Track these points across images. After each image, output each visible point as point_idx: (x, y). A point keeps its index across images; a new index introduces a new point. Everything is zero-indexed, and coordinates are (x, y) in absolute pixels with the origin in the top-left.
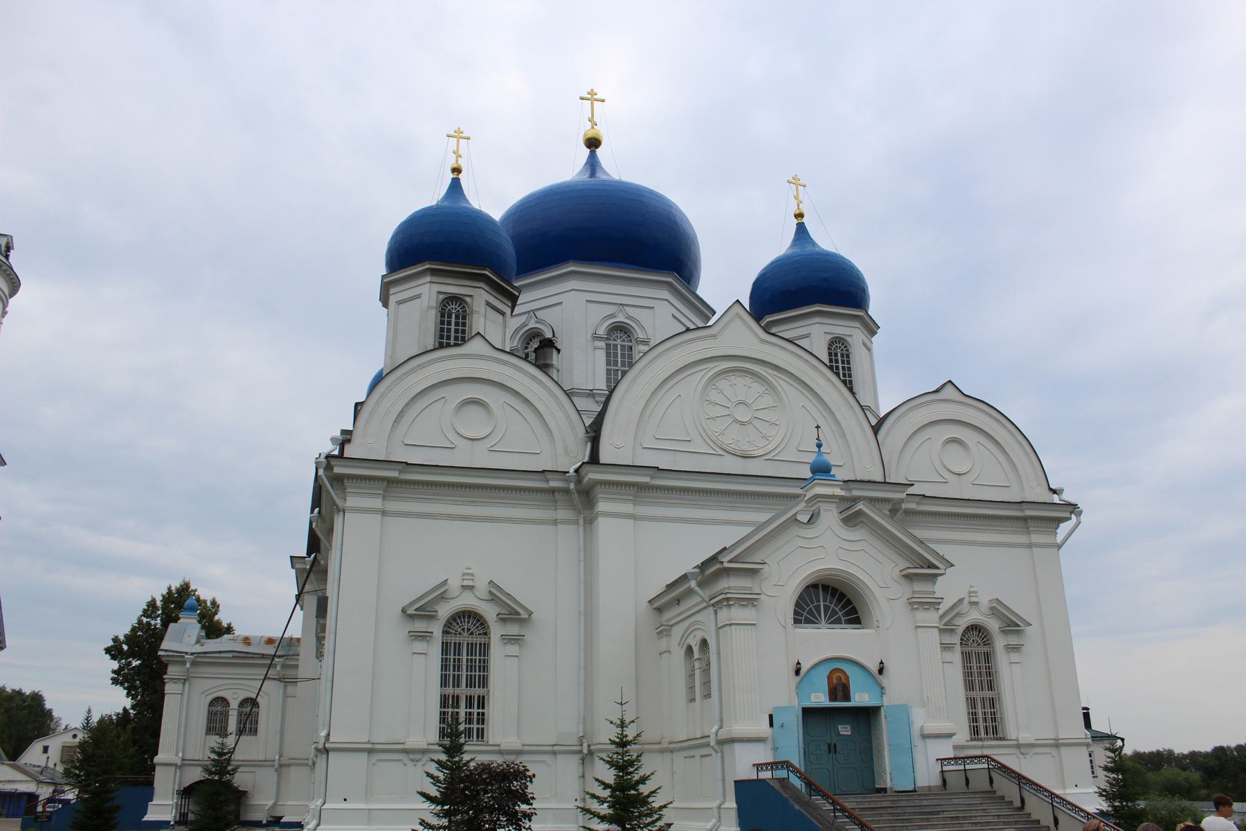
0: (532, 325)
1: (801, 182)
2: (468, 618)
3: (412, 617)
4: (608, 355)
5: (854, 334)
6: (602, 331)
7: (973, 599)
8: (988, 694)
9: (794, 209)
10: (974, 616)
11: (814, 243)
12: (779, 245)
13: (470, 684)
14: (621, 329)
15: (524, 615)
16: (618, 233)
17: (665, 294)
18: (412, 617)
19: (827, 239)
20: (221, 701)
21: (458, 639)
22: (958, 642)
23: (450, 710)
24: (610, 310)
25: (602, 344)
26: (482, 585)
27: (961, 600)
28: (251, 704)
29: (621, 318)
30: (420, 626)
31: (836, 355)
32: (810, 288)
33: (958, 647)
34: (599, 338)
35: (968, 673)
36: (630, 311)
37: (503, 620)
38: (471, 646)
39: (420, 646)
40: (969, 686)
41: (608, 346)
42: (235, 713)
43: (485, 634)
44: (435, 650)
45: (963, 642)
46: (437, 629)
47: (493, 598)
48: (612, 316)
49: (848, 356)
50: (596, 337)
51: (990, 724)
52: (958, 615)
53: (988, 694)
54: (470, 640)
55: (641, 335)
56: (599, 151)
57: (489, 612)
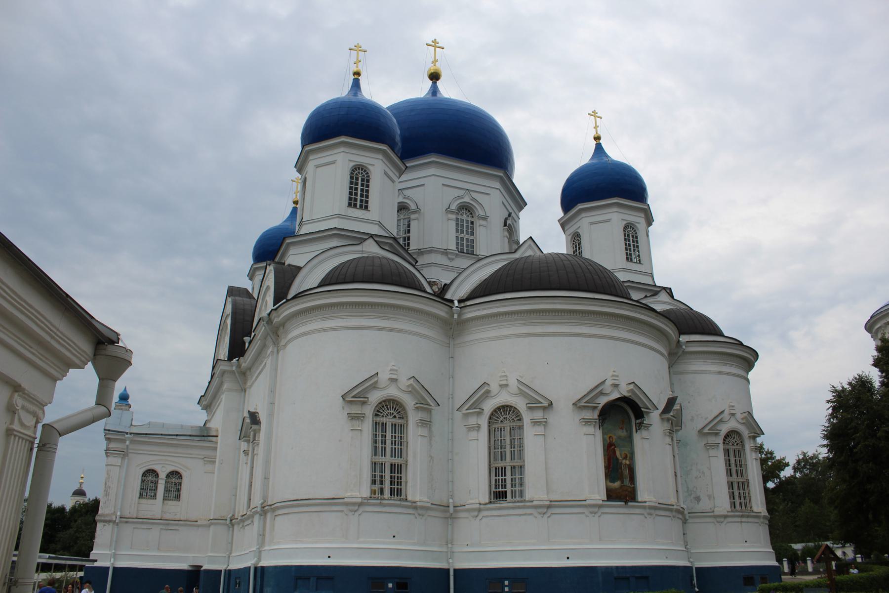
2: (391, 406)
3: (351, 402)
4: (457, 225)
6: (454, 207)
7: (732, 412)
9: (593, 133)
10: (732, 425)
11: (607, 156)
12: (582, 157)
13: (393, 454)
14: (466, 208)
16: (462, 139)
18: (351, 402)
19: (616, 153)
20: (151, 473)
21: (384, 420)
22: (721, 441)
25: (454, 217)
26: (404, 382)
27: (722, 412)
28: (175, 475)
29: (467, 199)
30: (356, 410)
32: (605, 185)
33: (721, 445)
34: (452, 212)
35: (728, 463)
36: (474, 195)
38: (394, 426)
39: (356, 424)
40: (729, 473)
41: (457, 219)
42: (164, 482)
44: (367, 427)
46: (369, 411)
47: (412, 391)
48: (461, 197)
50: (448, 210)
52: (721, 421)
53: (740, 479)
54: (395, 421)
55: (481, 213)
56: (439, 83)
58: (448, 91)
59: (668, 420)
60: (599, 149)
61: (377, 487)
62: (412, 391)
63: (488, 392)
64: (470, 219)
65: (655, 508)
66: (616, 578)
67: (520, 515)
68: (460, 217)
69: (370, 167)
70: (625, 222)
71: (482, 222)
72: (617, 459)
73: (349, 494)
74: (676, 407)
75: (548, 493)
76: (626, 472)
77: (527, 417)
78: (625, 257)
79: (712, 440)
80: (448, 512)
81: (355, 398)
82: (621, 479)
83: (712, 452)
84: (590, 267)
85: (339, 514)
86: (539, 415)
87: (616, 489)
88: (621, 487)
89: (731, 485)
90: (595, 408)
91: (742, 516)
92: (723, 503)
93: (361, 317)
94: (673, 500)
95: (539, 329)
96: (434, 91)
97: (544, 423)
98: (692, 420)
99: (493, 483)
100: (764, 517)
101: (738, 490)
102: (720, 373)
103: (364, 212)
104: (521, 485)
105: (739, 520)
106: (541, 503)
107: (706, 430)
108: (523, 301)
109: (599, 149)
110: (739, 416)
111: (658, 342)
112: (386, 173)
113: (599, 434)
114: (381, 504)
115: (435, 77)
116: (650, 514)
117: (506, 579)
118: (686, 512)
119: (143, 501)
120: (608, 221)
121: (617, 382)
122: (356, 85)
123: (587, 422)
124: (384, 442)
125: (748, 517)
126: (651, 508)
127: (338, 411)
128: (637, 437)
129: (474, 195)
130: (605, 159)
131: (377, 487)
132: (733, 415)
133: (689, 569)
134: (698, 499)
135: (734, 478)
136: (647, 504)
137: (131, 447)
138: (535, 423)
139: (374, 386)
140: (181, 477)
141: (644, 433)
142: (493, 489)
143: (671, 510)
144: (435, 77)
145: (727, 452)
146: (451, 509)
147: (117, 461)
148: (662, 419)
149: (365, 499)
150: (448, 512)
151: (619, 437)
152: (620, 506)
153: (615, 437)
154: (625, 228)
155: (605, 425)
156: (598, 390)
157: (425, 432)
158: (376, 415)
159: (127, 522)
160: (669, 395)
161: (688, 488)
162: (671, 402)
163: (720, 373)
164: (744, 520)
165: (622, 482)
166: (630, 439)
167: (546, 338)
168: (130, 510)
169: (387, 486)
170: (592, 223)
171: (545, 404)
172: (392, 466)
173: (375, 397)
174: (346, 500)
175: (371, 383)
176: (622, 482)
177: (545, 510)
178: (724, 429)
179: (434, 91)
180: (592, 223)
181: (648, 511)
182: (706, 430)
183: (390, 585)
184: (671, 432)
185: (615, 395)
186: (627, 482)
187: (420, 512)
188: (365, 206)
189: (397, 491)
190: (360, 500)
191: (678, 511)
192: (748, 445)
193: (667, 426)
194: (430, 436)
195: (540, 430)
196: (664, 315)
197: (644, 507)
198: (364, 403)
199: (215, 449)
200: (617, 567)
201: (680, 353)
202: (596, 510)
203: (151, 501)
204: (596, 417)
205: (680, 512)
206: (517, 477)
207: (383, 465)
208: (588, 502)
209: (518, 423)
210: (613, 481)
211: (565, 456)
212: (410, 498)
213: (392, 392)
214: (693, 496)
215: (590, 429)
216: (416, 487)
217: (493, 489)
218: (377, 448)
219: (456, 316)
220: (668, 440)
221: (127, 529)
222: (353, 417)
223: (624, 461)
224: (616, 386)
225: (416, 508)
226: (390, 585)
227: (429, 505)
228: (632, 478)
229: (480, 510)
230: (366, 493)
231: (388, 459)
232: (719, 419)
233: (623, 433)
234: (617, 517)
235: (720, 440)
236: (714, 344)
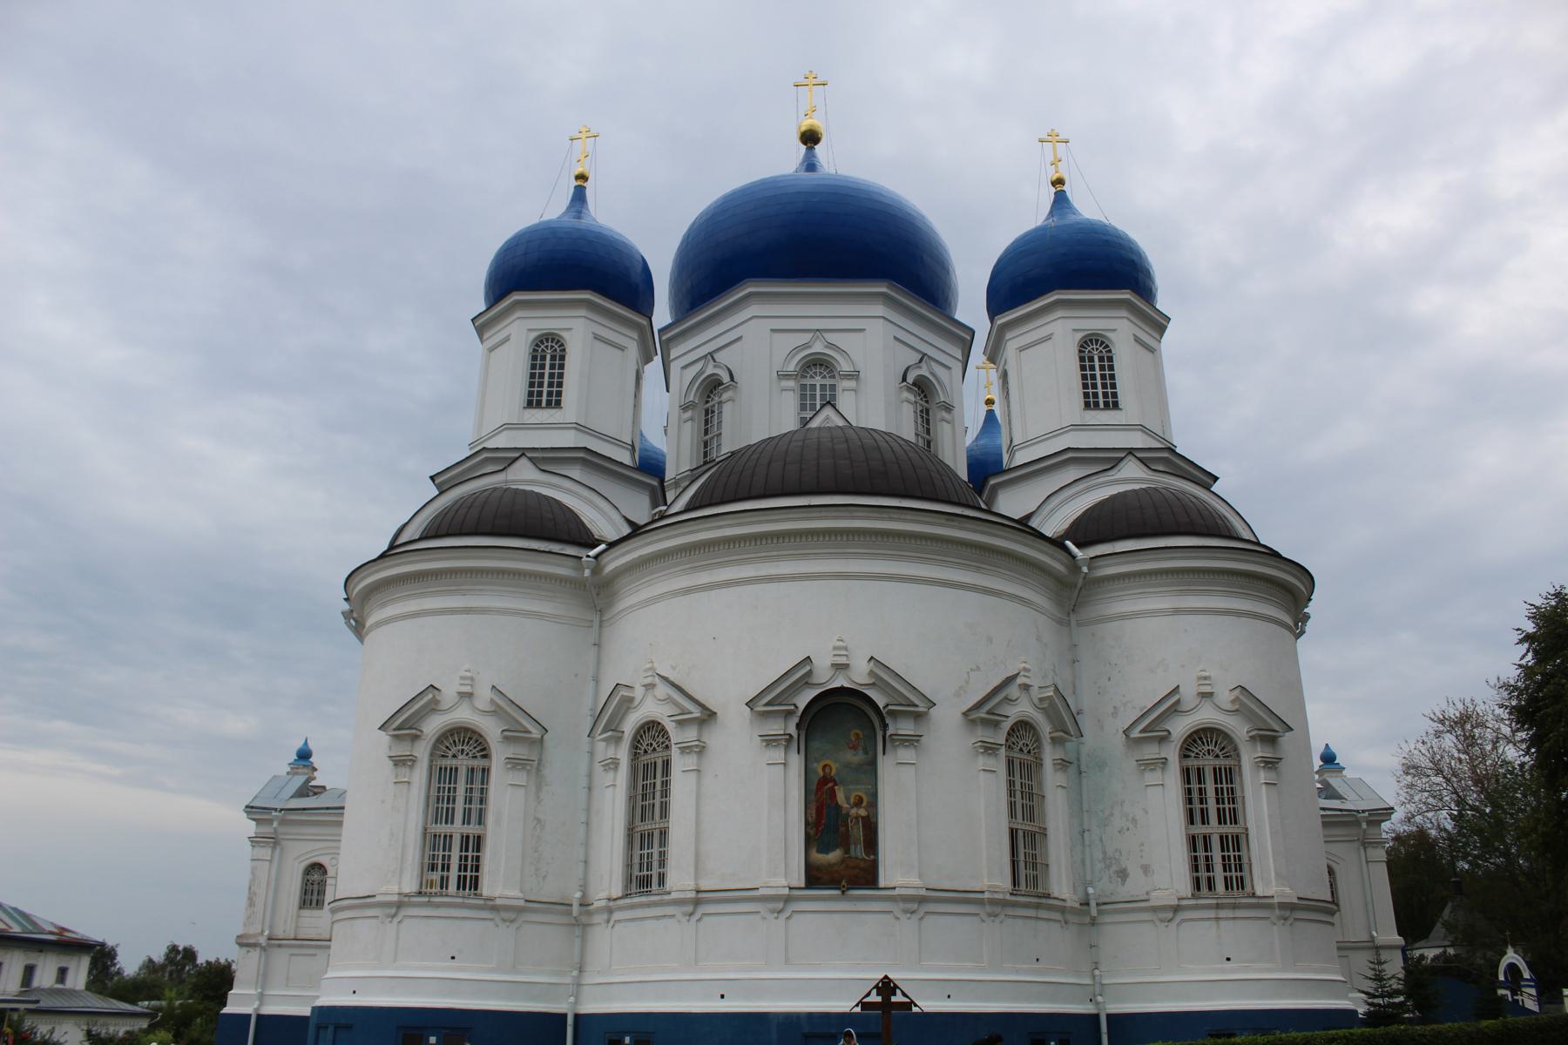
0: (709, 371)
1: (1061, 137)
2: (464, 738)
4: (803, 397)
5: (1121, 330)
6: (792, 367)
14: (817, 364)
15: (536, 733)
17: (879, 309)
21: (454, 762)
23: (470, 854)
24: (805, 338)
25: (791, 383)
26: (484, 695)
29: (818, 347)
30: (403, 749)
31: (1091, 359)
34: (787, 376)
36: (831, 337)
37: (507, 739)
41: (803, 387)
43: (485, 756)
44: (419, 776)
45: (1185, 753)
46: (422, 751)
47: (496, 712)
49: (1110, 359)
51: (1203, 874)
57: (491, 730)
58: (836, 162)
61: (436, 876)
63: (435, 701)
64: (828, 382)
65: (922, 900)
66: (806, 1036)
67: (658, 918)
68: (808, 382)
69: (564, 334)
70: (1080, 335)
72: (838, 807)
73: (383, 889)
75: (697, 877)
76: (858, 832)
77: (675, 735)
78: (1082, 400)
79: (1151, 751)
80: (576, 916)
81: (403, 726)
82: (845, 842)
83: (1153, 777)
84: (894, 444)
85: (373, 921)
86: (690, 734)
87: (831, 865)
88: (843, 861)
90: (789, 714)
93: (422, 595)
95: (704, 578)
96: (810, 165)
97: (700, 750)
98: (1115, 714)
99: (636, 860)
102: (1177, 611)
103: (552, 411)
104: (662, 863)
106: (682, 895)
107: (1135, 734)
110: (1225, 697)
111: (967, 567)
112: (597, 337)
113: (796, 762)
114: (429, 904)
115: (810, 138)
116: (905, 911)
117: (627, 1033)
119: (306, 913)
120: (1049, 338)
122: (579, 196)
123: (769, 741)
129: (831, 337)
130: (1071, 219)
131: (436, 876)
132: (1207, 696)
134: (1123, 874)
135: (1214, 828)
136: (987, 895)
137: (281, 830)
138: (685, 750)
140: (325, 872)
142: (636, 872)
143: (981, 902)
144: (810, 138)
145: (1186, 773)
146: (576, 909)
147: (265, 853)
149: (406, 895)
150: (576, 916)
151: (848, 765)
152: (830, 898)
153: (834, 766)
155: (815, 744)
157: (520, 778)
159: (280, 946)
161: (1104, 853)
163: (1177, 611)
165: (847, 851)
166: (872, 766)
167: (783, 586)
168: (284, 928)
169: (454, 873)
170: (1022, 349)
171: (697, 713)
172: (465, 839)
175: (427, 700)
176: (847, 851)
177: (690, 909)
178: (1180, 728)
179: (810, 165)
180: (1022, 349)
181: (988, 908)
182: (1135, 734)
186: (858, 851)
187: (505, 915)
188: (555, 402)
189: (469, 881)
190: (395, 898)
194: (539, 788)
195: (690, 761)
198: (415, 738)
199: (340, 824)
200: (810, 1015)
201: (1080, 582)
202: (915, 906)
203: (316, 913)
204: (792, 730)
206: (655, 850)
207: (448, 838)
210: (825, 849)
211: (742, 805)
213: (463, 715)
214: (1114, 868)
215: (778, 754)
217: (636, 872)
218: (440, 806)
219: (587, 573)
221: (280, 957)
222: (399, 762)
223: (854, 811)
225: (495, 908)
227: (522, 903)
228: (871, 843)
229: (399, 905)
230: (410, 885)
231: (457, 828)
232: (1171, 706)
233: (856, 758)
235: (1172, 753)
236: (1152, 555)
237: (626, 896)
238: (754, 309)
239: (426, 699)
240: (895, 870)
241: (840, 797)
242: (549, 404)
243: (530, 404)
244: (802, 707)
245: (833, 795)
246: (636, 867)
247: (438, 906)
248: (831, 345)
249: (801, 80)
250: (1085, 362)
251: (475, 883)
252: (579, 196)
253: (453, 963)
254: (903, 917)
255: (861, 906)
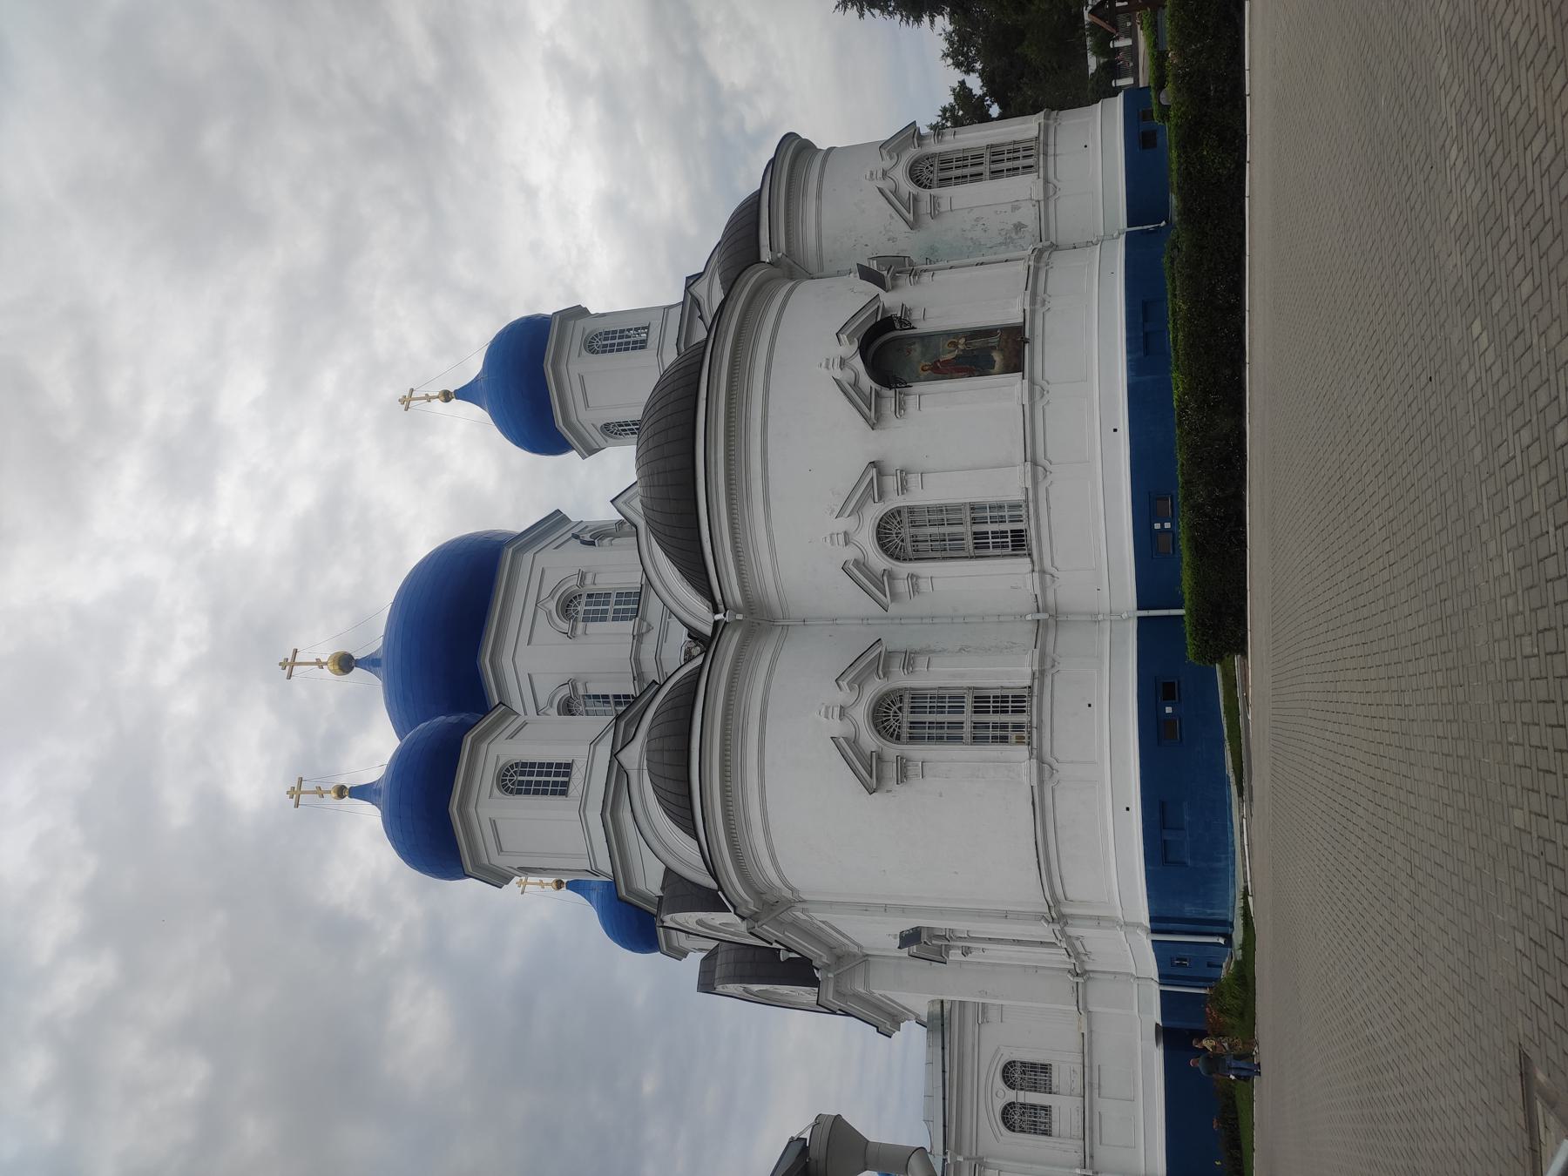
2: (884, 716)
4: (594, 620)
6: (565, 626)
8: (986, 159)
11: (476, 380)
13: (959, 709)
14: (567, 607)
21: (905, 725)
22: (928, 191)
25: (581, 625)
26: (844, 696)
27: (880, 190)
29: (552, 605)
30: (891, 771)
32: (526, 383)
33: (934, 191)
34: (574, 628)
35: (962, 179)
36: (544, 595)
38: (914, 710)
39: (913, 770)
40: (977, 177)
44: (917, 752)
46: (892, 750)
47: (859, 683)
48: (549, 614)
50: (571, 635)
52: (895, 192)
53: (986, 159)
54: (906, 709)
55: (574, 581)
56: (357, 656)
58: (373, 638)
59: (894, 278)
60: (465, 394)
61: (1012, 735)
62: (859, 683)
63: (856, 563)
64: (584, 599)
66: (1146, 354)
67: (1049, 508)
68: (581, 615)
70: (584, 352)
71: (589, 580)
73: (1025, 779)
74: (874, 265)
76: (978, 343)
77: (895, 501)
79: (925, 207)
80: (1047, 621)
81: (872, 773)
83: (945, 206)
85: (1057, 793)
86: (891, 483)
88: (1001, 350)
89: (996, 174)
90: (878, 394)
91: (1045, 154)
92: (1024, 187)
94: (1021, 268)
96: (370, 663)
97: (904, 473)
99: (998, 552)
100: (1047, 117)
101: (1005, 162)
102: (819, 196)
104: (1001, 507)
105: (1051, 159)
108: (714, 512)
109: (465, 394)
111: (772, 297)
113: (918, 388)
114: (1039, 728)
116: (1043, 304)
118: (1040, 246)
120: (582, 378)
121: (837, 361)
122: (360, 792)
123: (900, 407)
124: (940, 725)
125: (1046, 144)
126: (1033, 302)
127: (895, 799)
128: (923, 327)
131: (1012, 735)
132: (885, 173)
133: (1129, 236)
134: (1019, 227)
135: (985, 169)
136: (1027, 308)
138: (904, 488)
139: (854, 742)
141: (916, 315)
142: (1009, 551)
143: (1037, 270)
144: (345, 663)
145: (944, 182)
146: (1041, 616)
148: (893, 288)
149: (1031, 753)
150: (1047, 621)
154: (593, 351)
155: (905, 378)
156: (850, 391)
157: (921, 661)
158: (898, 738)
160: (854, 278)
162: (867, 274)
163: (819, 196)
164: (1051, 151)
165: (993, 348)
166: (926, 338)
170: (587, 405)
173: (870, 741)
174: (1035, 784)
175: (848, 748)
176: (993, 348)
178: (907, 187)
179: (370, 663)
180: (587, 405)
181: (1038, 306)
182: (910, 217)
183: (1169, 710)
184: (915, 273)
185: (858, 363)
186: (994, 340)
188: (566, 769)
189: (1015, 702)
191: (1038, 259)
192: (933, 147)
193: (904, 280)
194: (930, 652)
195: (914, 480)
196: (730, 288)
197: (1033, 312)
198: (880, 758)
200: (1129, 352)
202: (1037, 388)
205: (1039, 254)
207: (976, 726)
208: (1026, 402)
209: (905, 515)
210: (991, 363)
211: (955, 439)
212: (1028, 682)
213: (861, 714)
215: (912, 401)
216: (1012, 673)
217: (1009, 551)
220: (926, 277)
222: (903, 776)
224: (843, 363)
225: (1042, 672)
226: (1169, 710)
227: (1037, 651)
229: (1043, 572)
230: (1023, 751)
231: (967, 717)
232: (890, 196)
233: (917, 350)
234: (1048, 355)
235: (925, 194)
237: (1030, 555)
238: (506, 662)
239: (845, 745)
240: (1010, 314)
241: (949, 357)
242: (567, 774)
243: (562, 790)
244: (875, 386)
245: (947, 362)
246: (1006, 551)
247: (1040, 721)
248: (552, 594)
249: (286, 671)
250: (606, 350)
251: (1018, 699)
252: (360, 792)
253: (1094, 705)
254: (1048, 305)
255: (1038, 331)
